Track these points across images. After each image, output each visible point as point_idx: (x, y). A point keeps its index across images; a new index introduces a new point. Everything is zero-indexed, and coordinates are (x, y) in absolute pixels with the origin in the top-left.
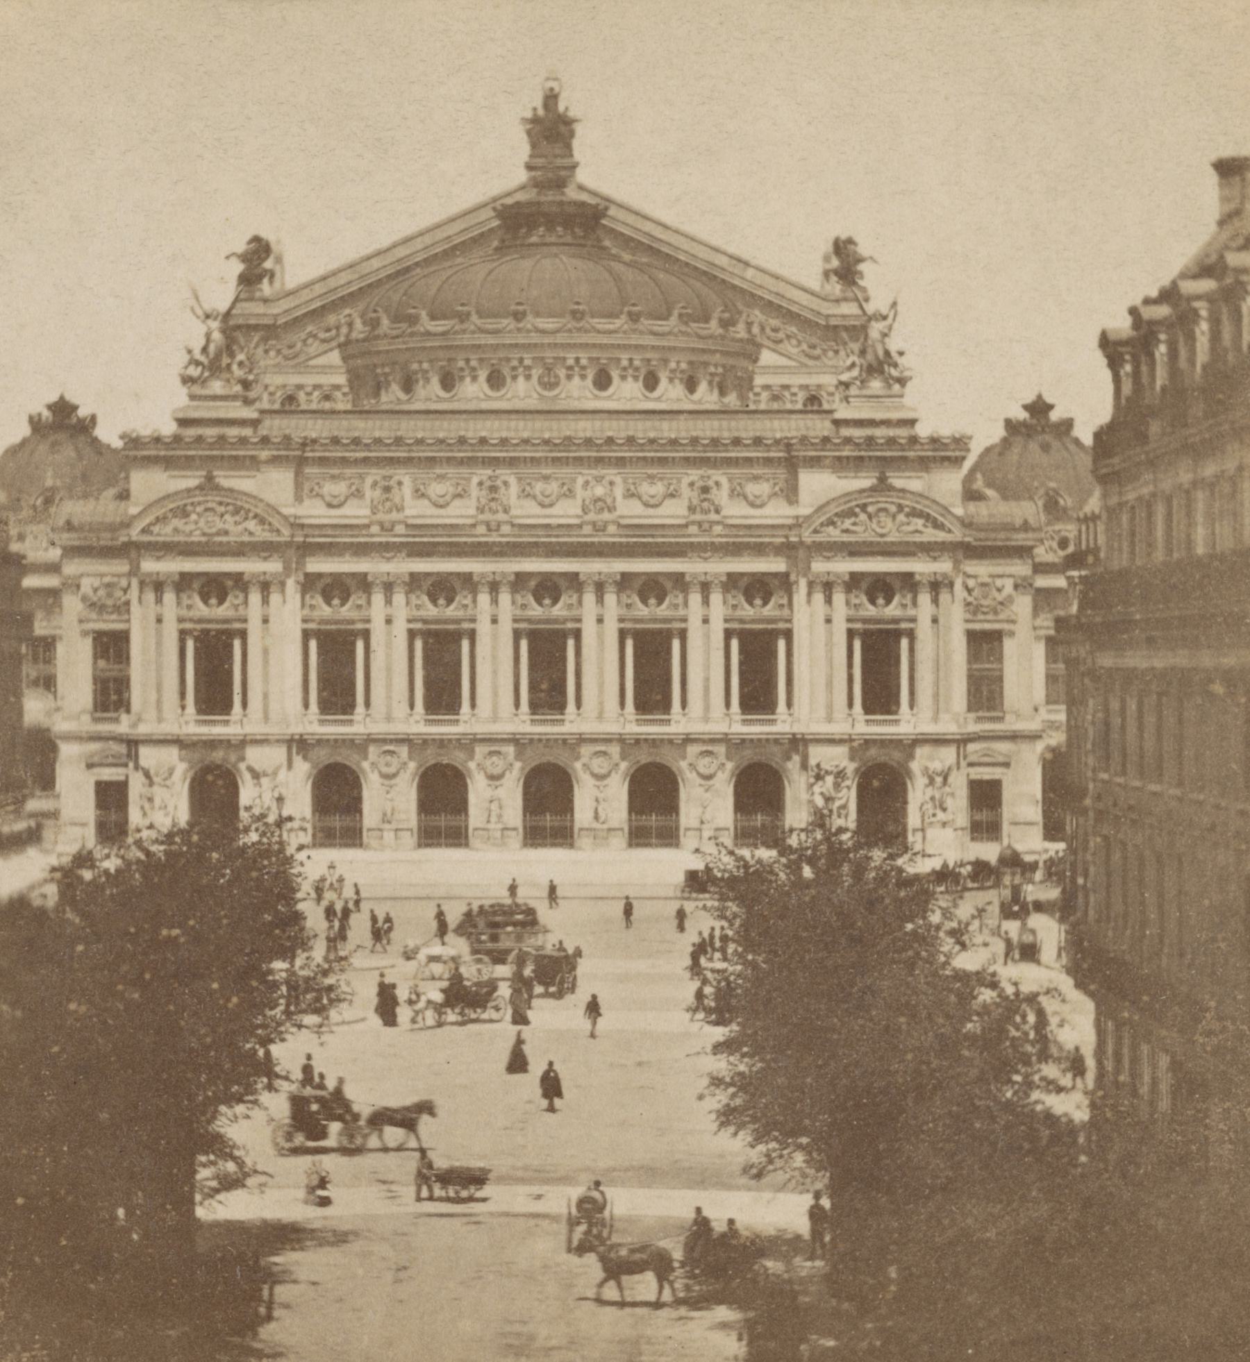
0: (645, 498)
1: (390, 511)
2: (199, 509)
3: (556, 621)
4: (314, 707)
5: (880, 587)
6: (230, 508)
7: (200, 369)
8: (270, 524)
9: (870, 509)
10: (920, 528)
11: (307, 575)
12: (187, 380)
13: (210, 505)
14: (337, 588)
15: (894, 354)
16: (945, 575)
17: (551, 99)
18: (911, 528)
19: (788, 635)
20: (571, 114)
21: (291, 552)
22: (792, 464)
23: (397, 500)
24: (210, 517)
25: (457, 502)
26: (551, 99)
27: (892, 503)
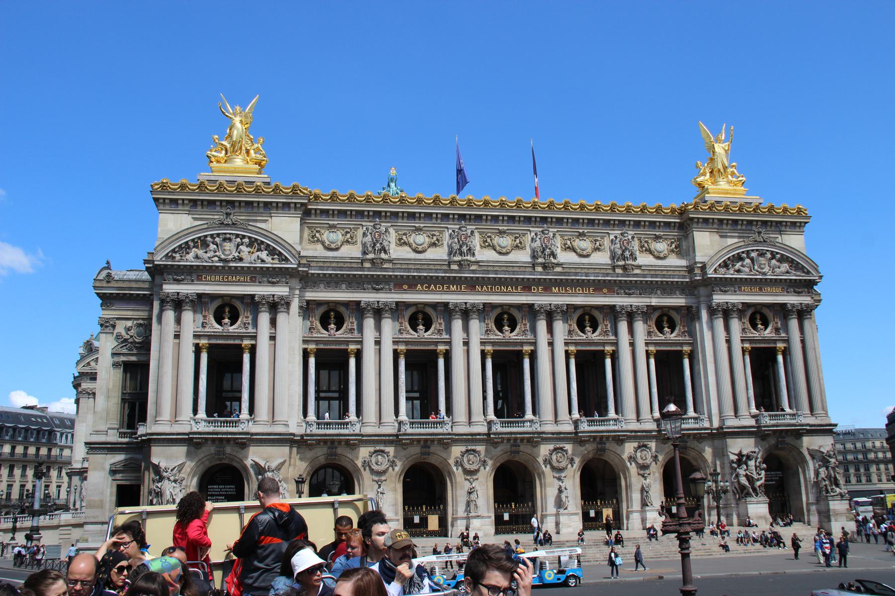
0: (578, 251)
1: (380, 251)
2: (217, 239)
3: (515, 344)
5: (757, 315)
6: (246, 240)
7: (224, 152)
8: (280, 254)
11: (308, 302)
13: (228, 236)
14: (331, 315)
16: (807, 305)
19: (692, 356)
21: (295, 283)
23: (385, 243)
24: (228, 246)
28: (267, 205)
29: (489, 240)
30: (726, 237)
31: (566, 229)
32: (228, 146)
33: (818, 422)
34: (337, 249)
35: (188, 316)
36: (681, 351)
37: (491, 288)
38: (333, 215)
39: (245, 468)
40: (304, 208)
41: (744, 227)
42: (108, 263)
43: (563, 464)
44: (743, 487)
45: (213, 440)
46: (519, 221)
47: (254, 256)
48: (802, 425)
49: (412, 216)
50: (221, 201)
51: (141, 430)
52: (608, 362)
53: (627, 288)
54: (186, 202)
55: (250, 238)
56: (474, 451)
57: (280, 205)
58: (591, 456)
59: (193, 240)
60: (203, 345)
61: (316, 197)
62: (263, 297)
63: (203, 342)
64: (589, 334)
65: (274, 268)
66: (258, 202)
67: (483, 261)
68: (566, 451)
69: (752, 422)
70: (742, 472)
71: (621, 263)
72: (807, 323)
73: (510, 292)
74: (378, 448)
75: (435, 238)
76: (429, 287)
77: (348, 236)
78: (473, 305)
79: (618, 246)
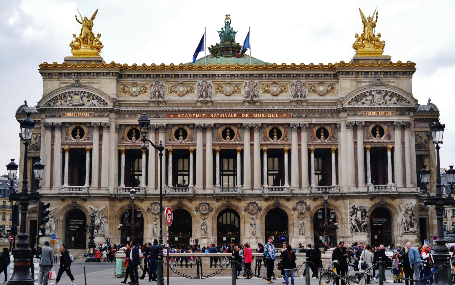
2: (71, 94)
4: (123, 185)
6: (86, 94)
9: (373, 93)
10: (396, 102)
11: (120, 125)
12: (73, 47)
13: (77, 92)
15: (376, 36)
17: (228, 24)
18: (392, 101)
19: (336, 152)
20: (233, 30)
21: (113, 115)
22: (335, 76)
23: (162, 93)
24: (76, 97)
26: (228, 24)
27: (383, 90)
28: (98, 74)
29: (220, 88)
30: (361, 82)
31: (265, 81)
32: (81, 41)
33: (407, 191)
34: (136, 96)
35: (58, 135)
36: (330, 149)
37: (219, 115)
38: (134, 77)
39: (87, 211)
40: (118, 75)
41: (373, 76)
42: (25, 102)
43: (255, 211)
44: (354, 226)
45: (70, 197)
46: (237, 77)
48: (394, 192)
49: (177, 76)
50: (74, 73)
52: (286, 155)
53: (299, 114)
54: (56, 74)
55: (88, 93)
56: (206, 203)
57: (105, 74)
58: (272, 208)
59: (59, 95)
60: (66, 149)
61: (124, 68)
62: (96, 124)
63: (66, 147)
64: (275, 140)
65: (100, 109)
66: (94, 73)
67: (216, 100)
68: (257, 204)
69: (366, 190)
70: (354, 218)
71: (295, 99)
72: (407, 133)
73: (229, 117)
74: (154, 202)
75: (189, 89)
76: (185, 115)
77: (142, 88)
78: (209, 125)
79: (294, 89)
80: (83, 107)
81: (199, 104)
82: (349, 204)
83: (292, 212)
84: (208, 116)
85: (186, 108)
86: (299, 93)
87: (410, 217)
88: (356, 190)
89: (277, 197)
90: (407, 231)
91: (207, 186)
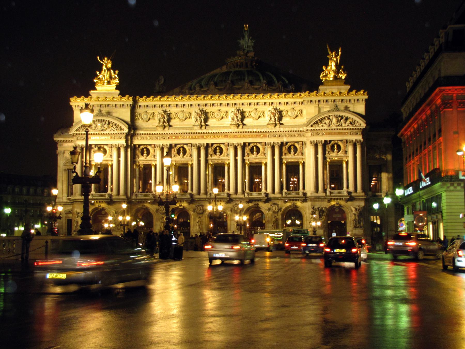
9: (331, 117)
11: (135, 145)
19: (303, 164)
25: (186, 120)
30: (323, 108)
33: (357, 195)
47: (111, 129)
51: (72, 198)
80: (105, 132)
81: (195, 128)
82: (311, 205)
83: (268, 212)
84: (203, 137)
85: (185, 131)
86: (273, 117)
87: (358, 216)
88: (316, 195)
89: (255, 200)
90: (355, 227)
91: (202, 191)
